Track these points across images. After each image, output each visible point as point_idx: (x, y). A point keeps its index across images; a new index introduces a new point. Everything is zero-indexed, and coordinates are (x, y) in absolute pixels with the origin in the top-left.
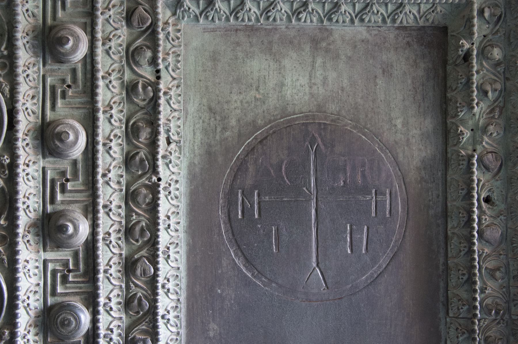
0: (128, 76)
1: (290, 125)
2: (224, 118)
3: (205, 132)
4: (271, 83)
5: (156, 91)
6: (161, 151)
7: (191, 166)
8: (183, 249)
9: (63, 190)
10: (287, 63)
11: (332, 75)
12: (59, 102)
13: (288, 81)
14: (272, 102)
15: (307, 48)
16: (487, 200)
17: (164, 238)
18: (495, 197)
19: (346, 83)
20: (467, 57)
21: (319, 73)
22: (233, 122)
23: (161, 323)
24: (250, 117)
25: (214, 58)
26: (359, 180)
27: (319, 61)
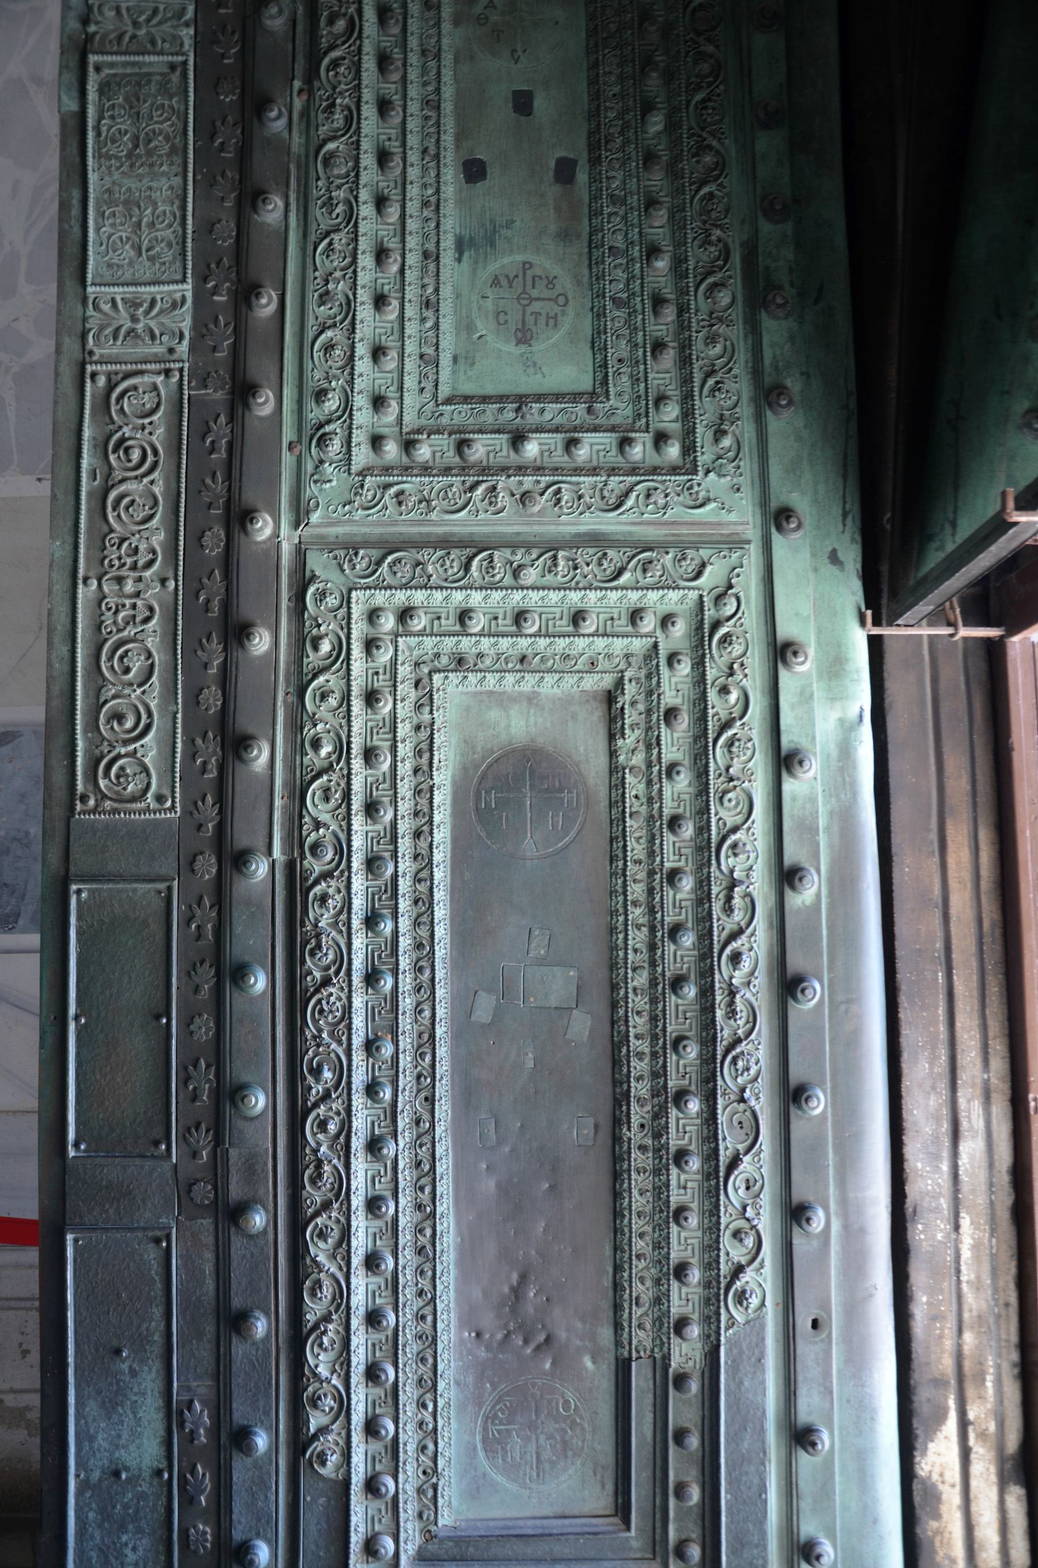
0: (415, 721)
1: (514, 751)
2: (474, 747)
3: (462, 755)
4: (503, 725)
5: (432, 730)
6: (435, 766)
7: (453, 776)
8: (448, 826)
9: (377, 789)
10: (512, 712)
11: (540, 720)
12: (375, 737)
13: (513, 723)
14: (503, 736)
15: (525, 704)
16: (636, 797)
17: (437, 818)
18: (640, 795)
19: (548, 725)
20: (622, 709)
21: (532, 720)
22: (479, 749)
23: (435, 870)
24: (489, 746)
25: (468, 709)
26: (557, 785)
27: (532, 712)
